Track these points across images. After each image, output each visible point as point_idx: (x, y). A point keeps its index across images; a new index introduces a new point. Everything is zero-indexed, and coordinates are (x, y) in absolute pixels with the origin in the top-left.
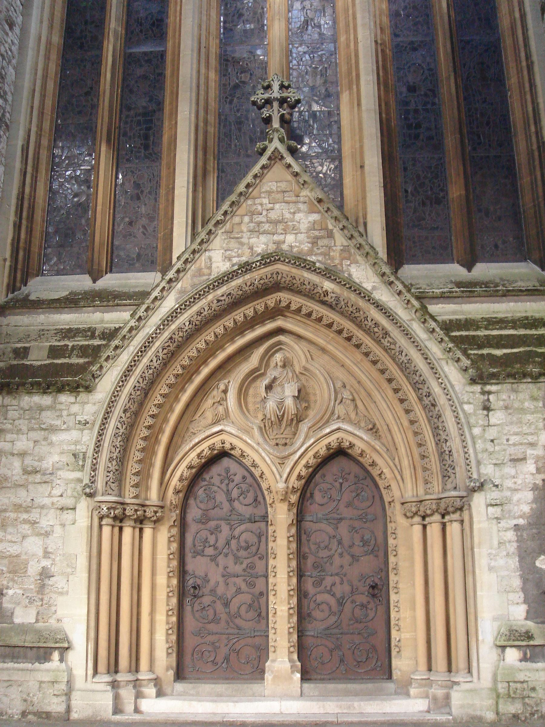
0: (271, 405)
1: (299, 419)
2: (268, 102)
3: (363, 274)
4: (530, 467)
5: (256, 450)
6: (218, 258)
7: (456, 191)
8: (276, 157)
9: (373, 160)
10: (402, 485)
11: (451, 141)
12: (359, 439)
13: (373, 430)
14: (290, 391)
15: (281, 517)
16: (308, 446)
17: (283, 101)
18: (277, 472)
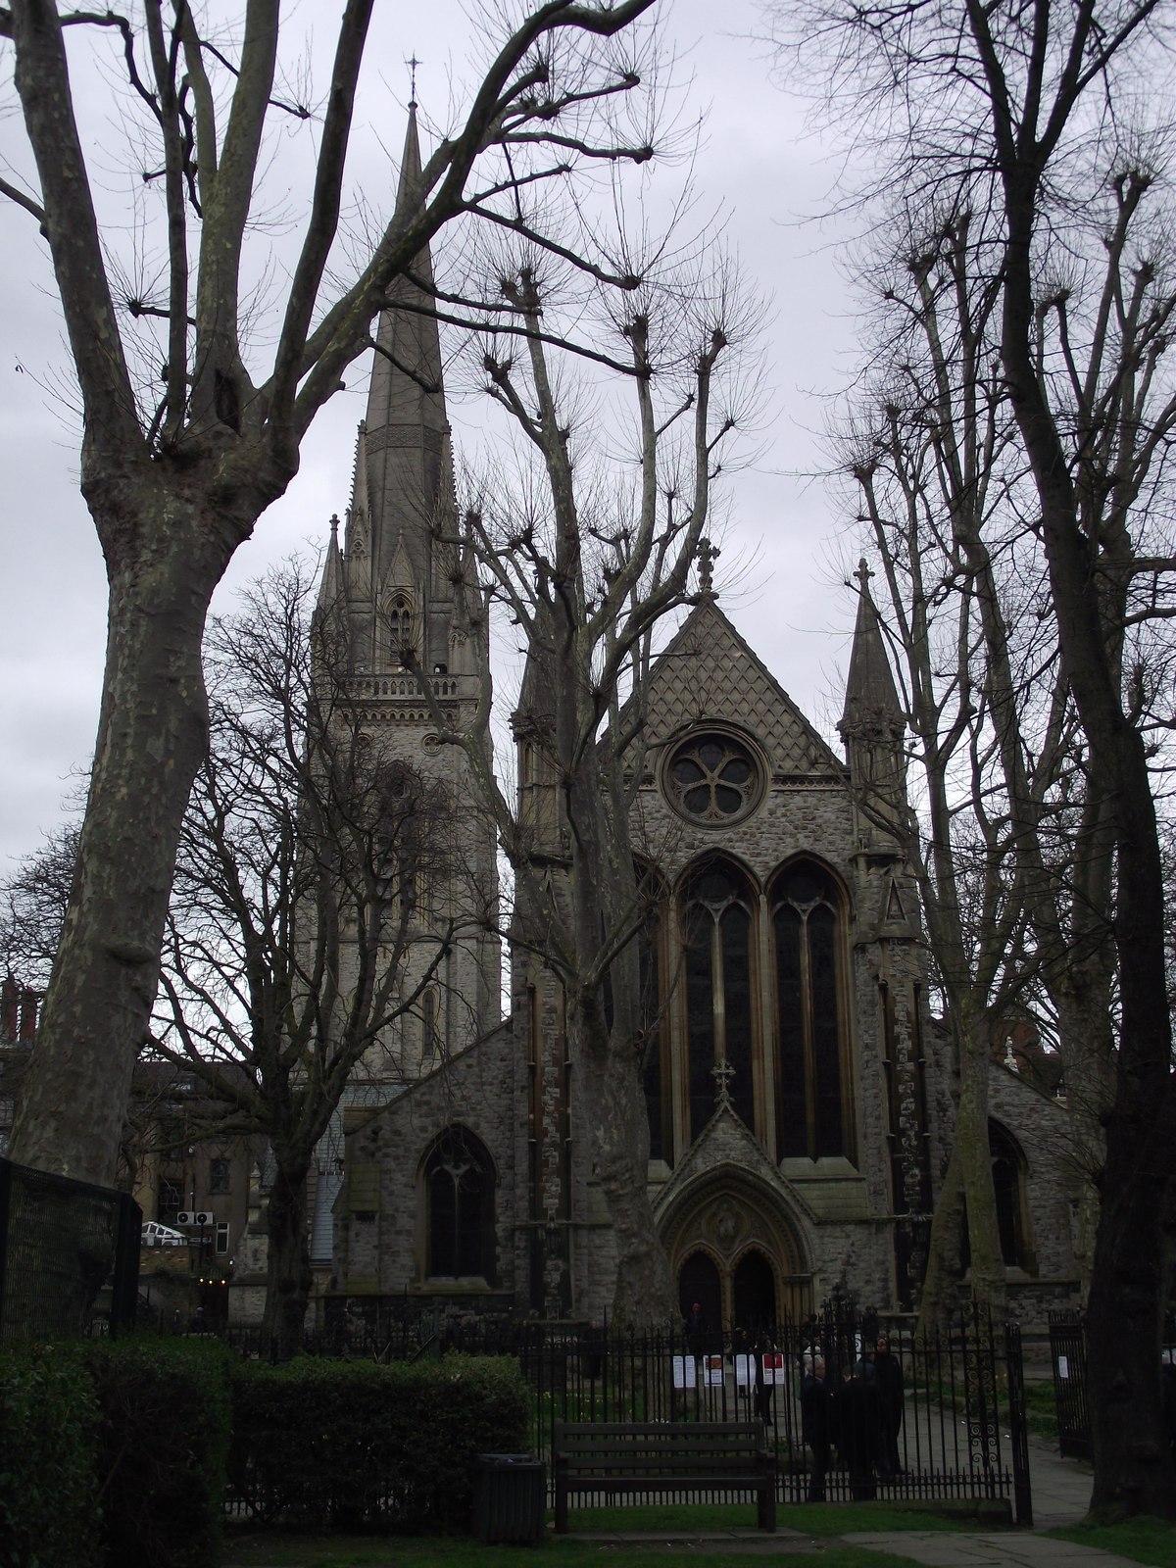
0: (722, 1229)
1: (733, 1238)
2: (720, 1075)
3: (765, 1173)
4: (839, 1262)
5: (715, 1250)
6: (702, 1165)
7: (810, 1118)
8: (726, 1110)
9: (771, 1107)
10: (782, 1270)
11: (808, 1089)
12: (762, 1245)
13: (769, 1242)
14: (730, 1224)
15: (728, 1284)
16: (738, 1249)
17: (727, 1076)
18: (727, 1265)
